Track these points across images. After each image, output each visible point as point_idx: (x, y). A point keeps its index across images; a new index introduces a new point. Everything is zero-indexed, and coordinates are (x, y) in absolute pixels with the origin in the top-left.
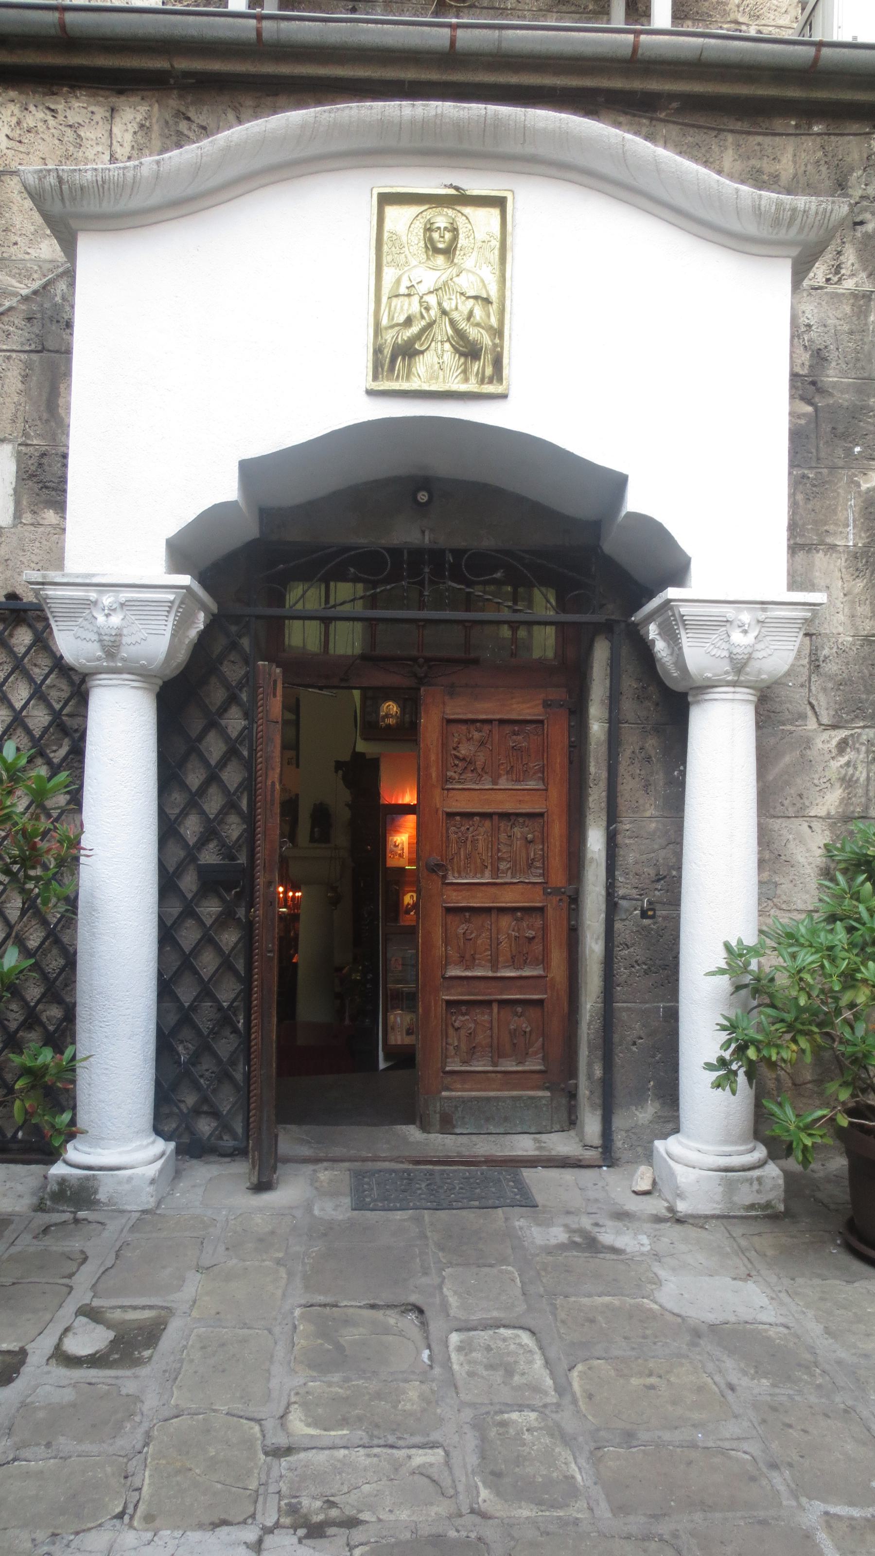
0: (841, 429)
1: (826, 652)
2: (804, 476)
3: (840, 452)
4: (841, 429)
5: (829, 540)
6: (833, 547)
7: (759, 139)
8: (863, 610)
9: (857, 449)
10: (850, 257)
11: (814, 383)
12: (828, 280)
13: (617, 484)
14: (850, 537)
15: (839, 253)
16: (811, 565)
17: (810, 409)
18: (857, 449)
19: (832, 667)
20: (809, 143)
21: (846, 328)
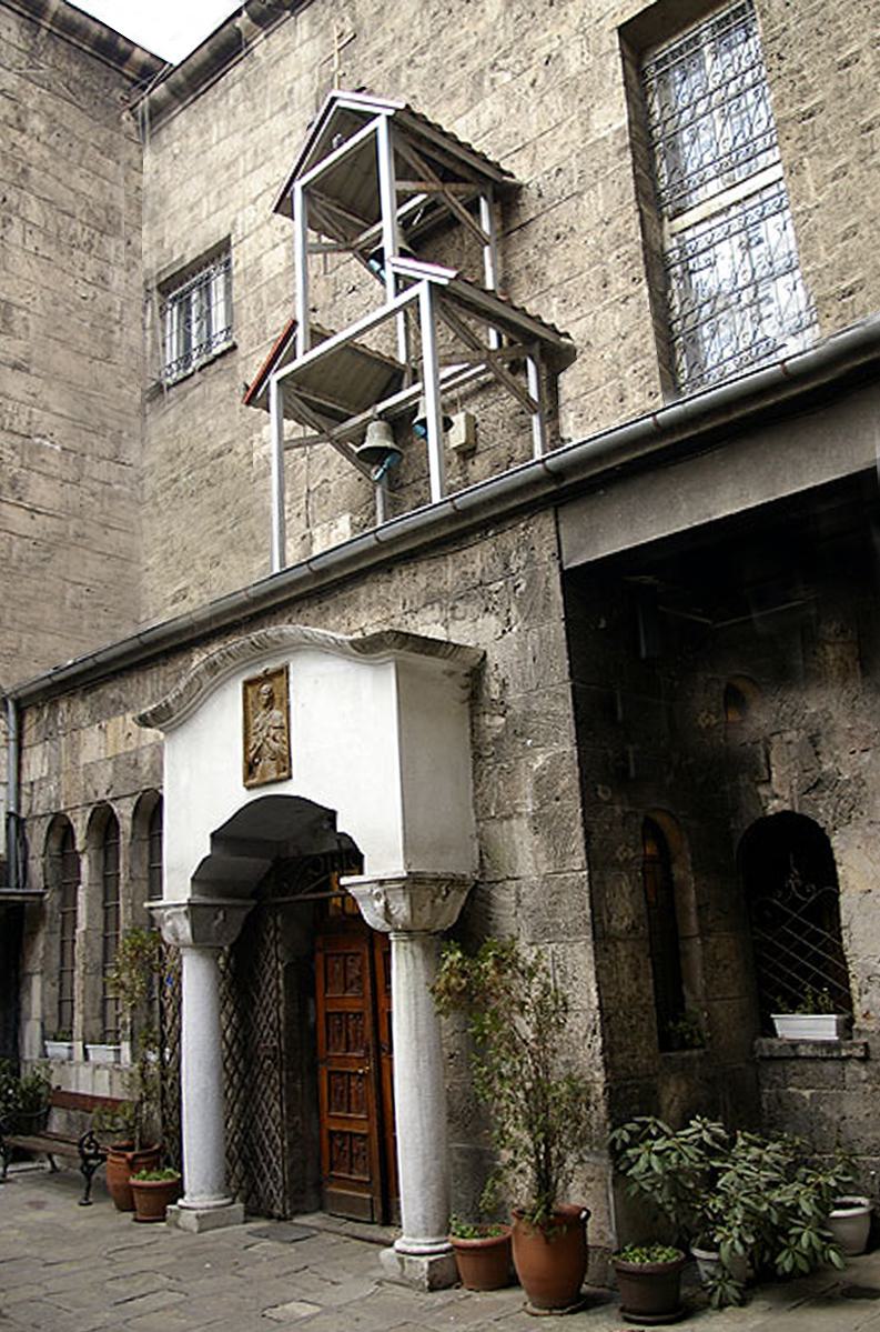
0: (519, 731)
1: (523, 890)
2: (502, 768)
3: (520, 746)
4: (519, 731)
5: (519, 810)
6: (520, 814)
7: (464, 552)
8: (542, 856)
9: (529, 742)
10: (514, 612)
11: (502, 703)
12: (504, 632)
13: (331, 816)
14: (529, 806)
15: (508, 610)
16: (511, 829)
17: (503, 720)
18: (529, 742)
19: (526, 901)
20: (488, 544)
21: (516, 659)
